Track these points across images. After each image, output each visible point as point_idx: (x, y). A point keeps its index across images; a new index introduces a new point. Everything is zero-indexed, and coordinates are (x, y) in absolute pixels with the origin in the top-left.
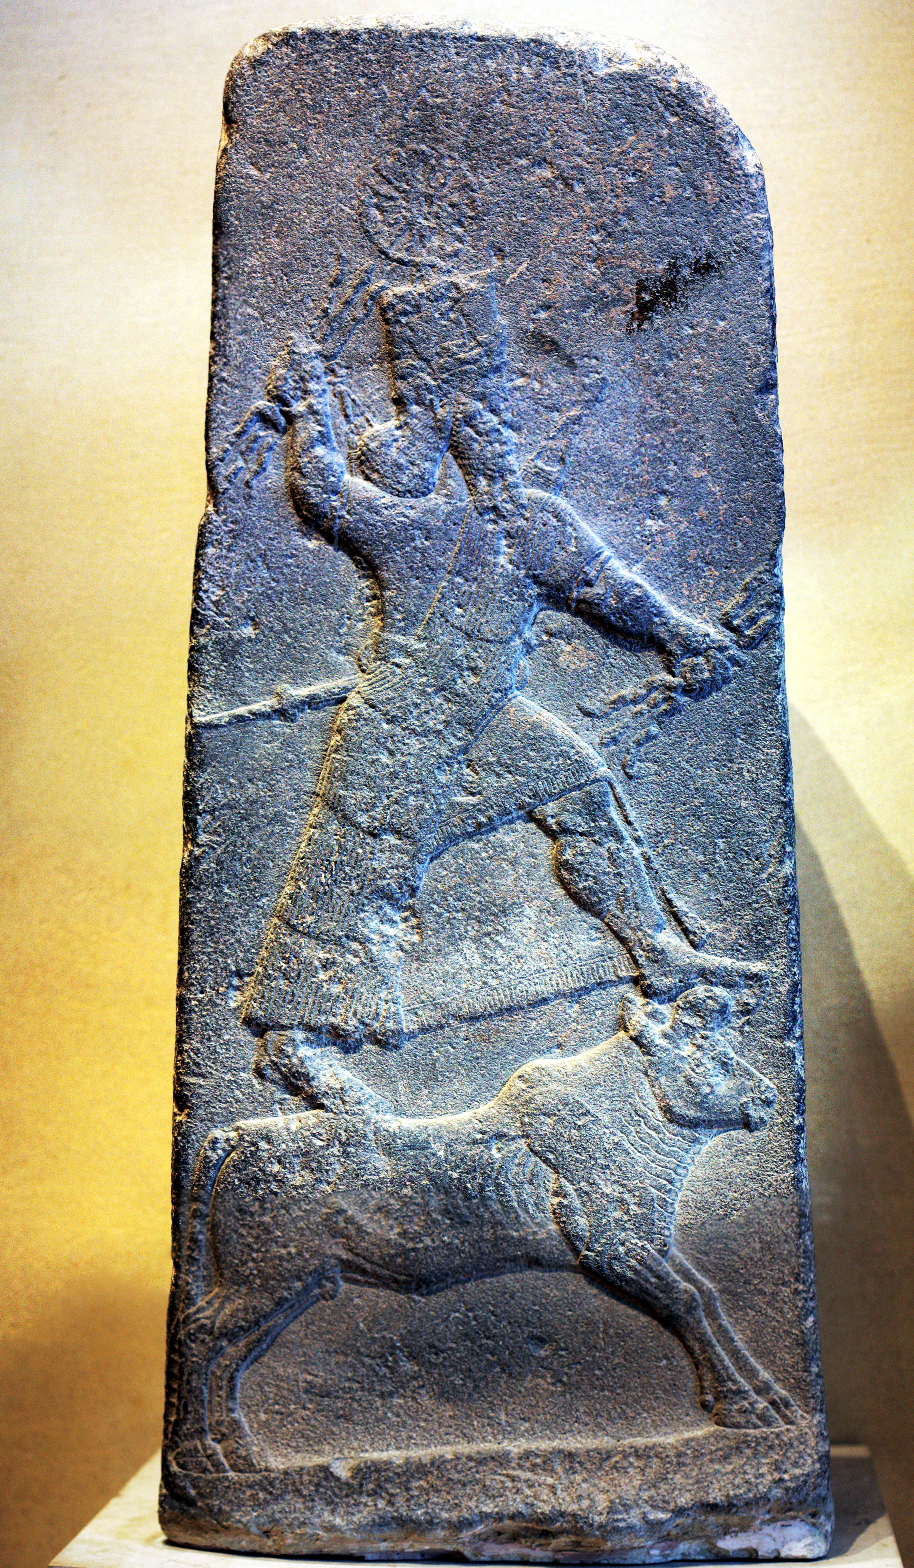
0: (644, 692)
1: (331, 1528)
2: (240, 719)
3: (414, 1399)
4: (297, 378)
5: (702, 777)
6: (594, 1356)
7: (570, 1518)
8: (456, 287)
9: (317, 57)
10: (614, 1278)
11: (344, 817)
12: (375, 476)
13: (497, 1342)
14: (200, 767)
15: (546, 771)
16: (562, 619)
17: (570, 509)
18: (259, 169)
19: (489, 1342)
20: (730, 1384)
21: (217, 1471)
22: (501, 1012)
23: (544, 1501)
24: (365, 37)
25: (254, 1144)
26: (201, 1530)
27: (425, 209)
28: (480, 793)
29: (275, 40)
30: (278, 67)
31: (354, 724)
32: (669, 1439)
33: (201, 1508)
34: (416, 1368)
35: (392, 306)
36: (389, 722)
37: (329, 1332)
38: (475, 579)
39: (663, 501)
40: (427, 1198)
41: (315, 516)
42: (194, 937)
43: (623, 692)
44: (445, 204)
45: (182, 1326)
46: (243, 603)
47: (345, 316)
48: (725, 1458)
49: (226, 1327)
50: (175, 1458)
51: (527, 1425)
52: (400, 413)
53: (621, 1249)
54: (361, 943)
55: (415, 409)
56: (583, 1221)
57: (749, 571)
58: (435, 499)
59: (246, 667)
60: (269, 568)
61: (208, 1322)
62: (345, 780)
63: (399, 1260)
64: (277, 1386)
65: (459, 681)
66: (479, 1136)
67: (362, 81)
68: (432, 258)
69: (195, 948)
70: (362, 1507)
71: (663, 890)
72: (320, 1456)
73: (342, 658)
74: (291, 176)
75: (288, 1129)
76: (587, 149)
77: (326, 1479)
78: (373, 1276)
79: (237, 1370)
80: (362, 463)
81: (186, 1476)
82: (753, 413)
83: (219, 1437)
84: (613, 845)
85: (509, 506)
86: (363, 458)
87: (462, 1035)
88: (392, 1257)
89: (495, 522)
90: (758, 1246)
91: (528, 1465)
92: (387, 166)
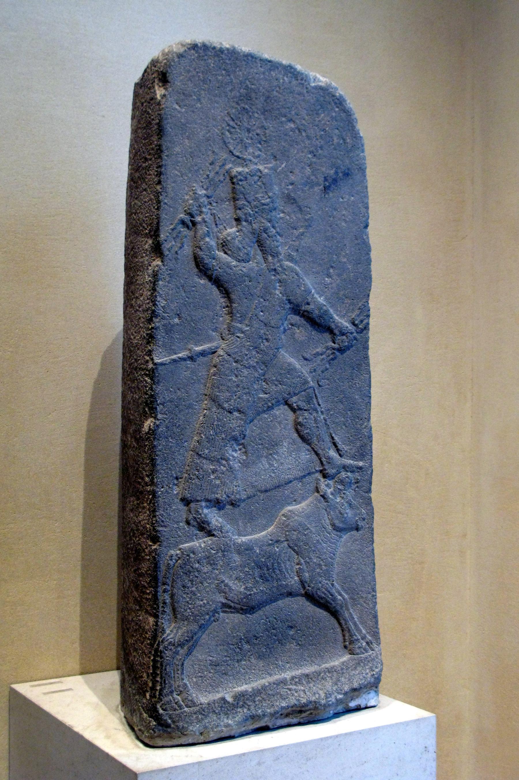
0: (324, 350)
1: (227, 726)
2: (174, 361)
3: (249, 661)
4: (197, 205)
5: (343, 386)
6: (309, 632)
7: (313, 703)
8: (260, 171)
9: (206, 57)
10: (318, 598)
11: (219, 405)
12: (229, 252)
13: (277, 631)
14: (157, 383)
15: (294, 384)
16: (296, 319)
17: (300, 272)
18: (180, 106)
19: (274, 631)
20: (354, 637)
21: (181, 709)
22: (275, 488)
23: (303, 698)
24: (226, 52)
25: (188, 555)
26: (172, 738)
27: (247, 134)
28: (269, 393)
29: (189, 46)
30: (190, 59)
31: (222, 363)
32: (336, 663)
33: (173, 728)
34: (249, 647)
35: (236, 176)
36: (236, 362)
37: (217, 636)
38: (268, 300)
39: (331, 271)
40: (254, 571)
41: (206, 269)
42: (158, 462)
43: (318, 350)
44: (255, 134)
45: (161, 643)
46: (175, 307)
47: (215, 179)
48: (356, 668)
49: (180, 641)
50: (161, 707)
51: (289, 665)
52: (237, 225)
53: (320, 585)
54: (226, 461)
55: (244, 223)
56: (307, 575)
57: (360, 301)
58: (252, 264)
59: (176, 337)
60: (185, 292)
61: (172, 640)
62: (219, 388)
63: (245, 600)
64: (199, 665)
65: (262, 344)
66: (271, 542)
67: (224, 72)
68: (250, 157)
69: (159, 467)
70: (238, 714)
71: (331, 433)
72: (219, 693)
73: (214, 333)
74: (193, 112)
75: (201, 547)
76: (307, 117)
77: (224, 703)
78: (233, 609)
79: (184, 660)
80: (223, 246)
81: (167, 714)
82: (362, 236)
83: (179, 693)
84: (315, 414)
85: (280, 269)
86: (224, 244)
87: (261, 498)
88: (242, 599)
89: (274, 275)
90: (361, 578)
91: (293, 682)
92: (233, 113)
